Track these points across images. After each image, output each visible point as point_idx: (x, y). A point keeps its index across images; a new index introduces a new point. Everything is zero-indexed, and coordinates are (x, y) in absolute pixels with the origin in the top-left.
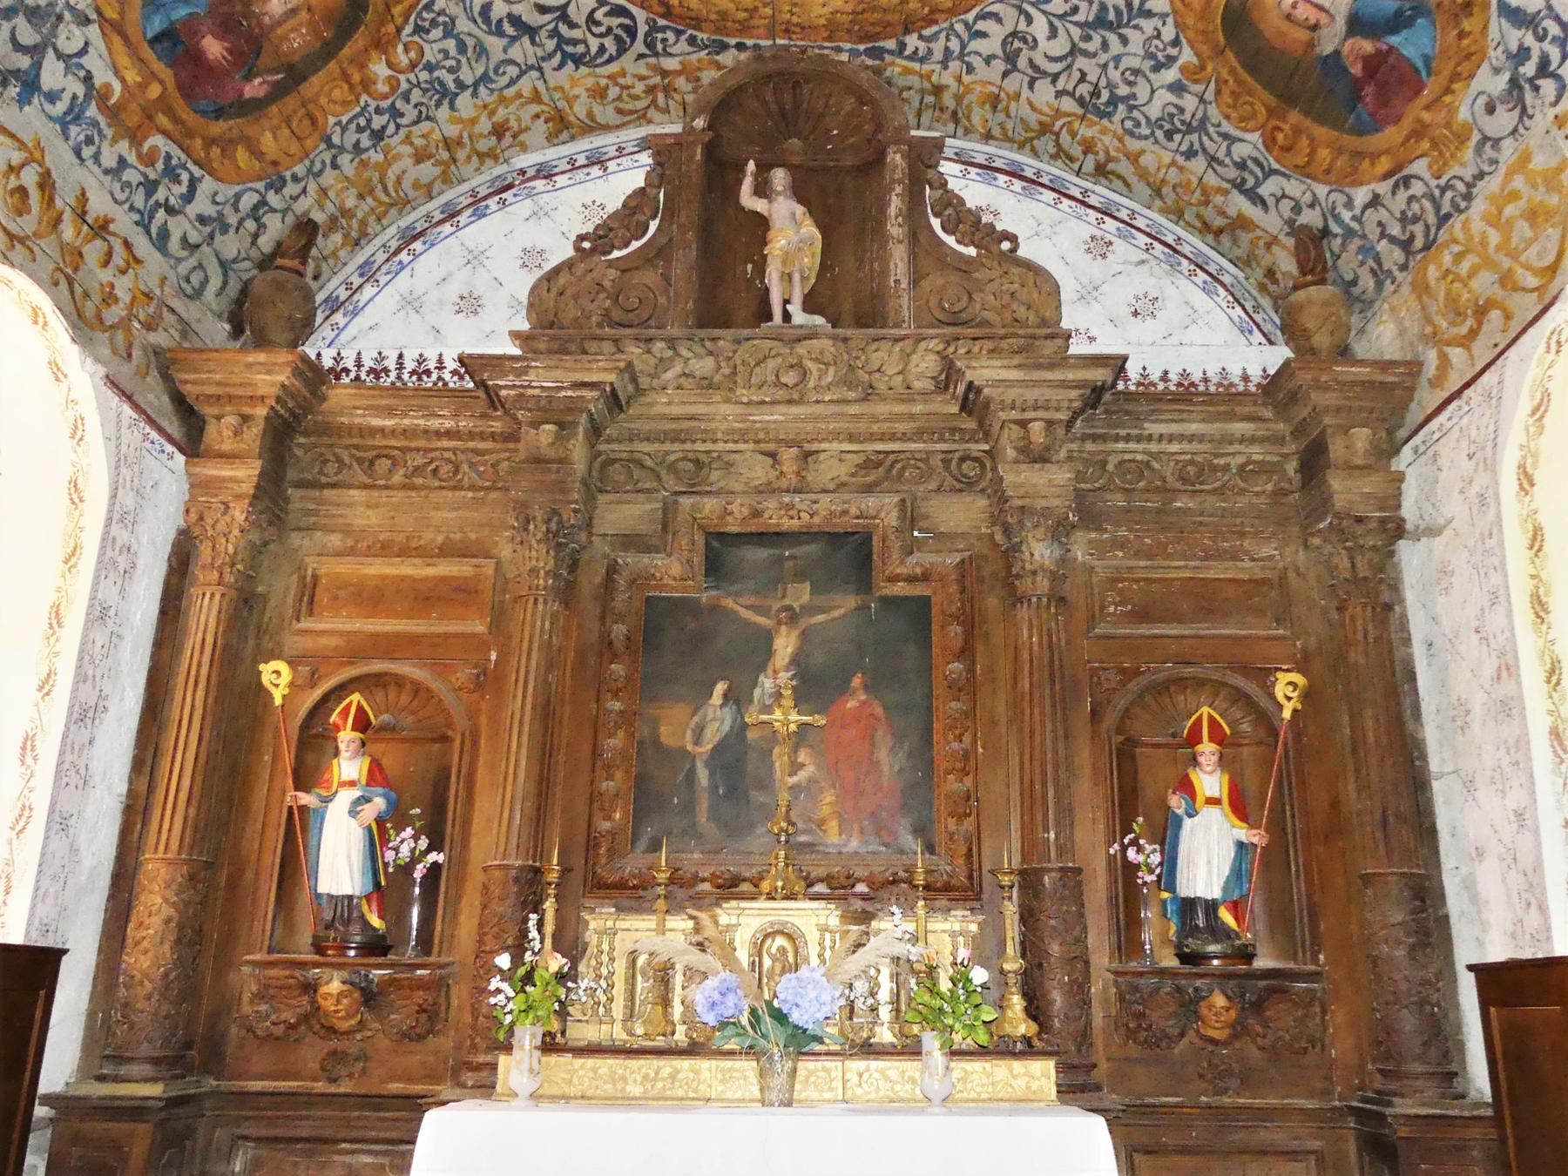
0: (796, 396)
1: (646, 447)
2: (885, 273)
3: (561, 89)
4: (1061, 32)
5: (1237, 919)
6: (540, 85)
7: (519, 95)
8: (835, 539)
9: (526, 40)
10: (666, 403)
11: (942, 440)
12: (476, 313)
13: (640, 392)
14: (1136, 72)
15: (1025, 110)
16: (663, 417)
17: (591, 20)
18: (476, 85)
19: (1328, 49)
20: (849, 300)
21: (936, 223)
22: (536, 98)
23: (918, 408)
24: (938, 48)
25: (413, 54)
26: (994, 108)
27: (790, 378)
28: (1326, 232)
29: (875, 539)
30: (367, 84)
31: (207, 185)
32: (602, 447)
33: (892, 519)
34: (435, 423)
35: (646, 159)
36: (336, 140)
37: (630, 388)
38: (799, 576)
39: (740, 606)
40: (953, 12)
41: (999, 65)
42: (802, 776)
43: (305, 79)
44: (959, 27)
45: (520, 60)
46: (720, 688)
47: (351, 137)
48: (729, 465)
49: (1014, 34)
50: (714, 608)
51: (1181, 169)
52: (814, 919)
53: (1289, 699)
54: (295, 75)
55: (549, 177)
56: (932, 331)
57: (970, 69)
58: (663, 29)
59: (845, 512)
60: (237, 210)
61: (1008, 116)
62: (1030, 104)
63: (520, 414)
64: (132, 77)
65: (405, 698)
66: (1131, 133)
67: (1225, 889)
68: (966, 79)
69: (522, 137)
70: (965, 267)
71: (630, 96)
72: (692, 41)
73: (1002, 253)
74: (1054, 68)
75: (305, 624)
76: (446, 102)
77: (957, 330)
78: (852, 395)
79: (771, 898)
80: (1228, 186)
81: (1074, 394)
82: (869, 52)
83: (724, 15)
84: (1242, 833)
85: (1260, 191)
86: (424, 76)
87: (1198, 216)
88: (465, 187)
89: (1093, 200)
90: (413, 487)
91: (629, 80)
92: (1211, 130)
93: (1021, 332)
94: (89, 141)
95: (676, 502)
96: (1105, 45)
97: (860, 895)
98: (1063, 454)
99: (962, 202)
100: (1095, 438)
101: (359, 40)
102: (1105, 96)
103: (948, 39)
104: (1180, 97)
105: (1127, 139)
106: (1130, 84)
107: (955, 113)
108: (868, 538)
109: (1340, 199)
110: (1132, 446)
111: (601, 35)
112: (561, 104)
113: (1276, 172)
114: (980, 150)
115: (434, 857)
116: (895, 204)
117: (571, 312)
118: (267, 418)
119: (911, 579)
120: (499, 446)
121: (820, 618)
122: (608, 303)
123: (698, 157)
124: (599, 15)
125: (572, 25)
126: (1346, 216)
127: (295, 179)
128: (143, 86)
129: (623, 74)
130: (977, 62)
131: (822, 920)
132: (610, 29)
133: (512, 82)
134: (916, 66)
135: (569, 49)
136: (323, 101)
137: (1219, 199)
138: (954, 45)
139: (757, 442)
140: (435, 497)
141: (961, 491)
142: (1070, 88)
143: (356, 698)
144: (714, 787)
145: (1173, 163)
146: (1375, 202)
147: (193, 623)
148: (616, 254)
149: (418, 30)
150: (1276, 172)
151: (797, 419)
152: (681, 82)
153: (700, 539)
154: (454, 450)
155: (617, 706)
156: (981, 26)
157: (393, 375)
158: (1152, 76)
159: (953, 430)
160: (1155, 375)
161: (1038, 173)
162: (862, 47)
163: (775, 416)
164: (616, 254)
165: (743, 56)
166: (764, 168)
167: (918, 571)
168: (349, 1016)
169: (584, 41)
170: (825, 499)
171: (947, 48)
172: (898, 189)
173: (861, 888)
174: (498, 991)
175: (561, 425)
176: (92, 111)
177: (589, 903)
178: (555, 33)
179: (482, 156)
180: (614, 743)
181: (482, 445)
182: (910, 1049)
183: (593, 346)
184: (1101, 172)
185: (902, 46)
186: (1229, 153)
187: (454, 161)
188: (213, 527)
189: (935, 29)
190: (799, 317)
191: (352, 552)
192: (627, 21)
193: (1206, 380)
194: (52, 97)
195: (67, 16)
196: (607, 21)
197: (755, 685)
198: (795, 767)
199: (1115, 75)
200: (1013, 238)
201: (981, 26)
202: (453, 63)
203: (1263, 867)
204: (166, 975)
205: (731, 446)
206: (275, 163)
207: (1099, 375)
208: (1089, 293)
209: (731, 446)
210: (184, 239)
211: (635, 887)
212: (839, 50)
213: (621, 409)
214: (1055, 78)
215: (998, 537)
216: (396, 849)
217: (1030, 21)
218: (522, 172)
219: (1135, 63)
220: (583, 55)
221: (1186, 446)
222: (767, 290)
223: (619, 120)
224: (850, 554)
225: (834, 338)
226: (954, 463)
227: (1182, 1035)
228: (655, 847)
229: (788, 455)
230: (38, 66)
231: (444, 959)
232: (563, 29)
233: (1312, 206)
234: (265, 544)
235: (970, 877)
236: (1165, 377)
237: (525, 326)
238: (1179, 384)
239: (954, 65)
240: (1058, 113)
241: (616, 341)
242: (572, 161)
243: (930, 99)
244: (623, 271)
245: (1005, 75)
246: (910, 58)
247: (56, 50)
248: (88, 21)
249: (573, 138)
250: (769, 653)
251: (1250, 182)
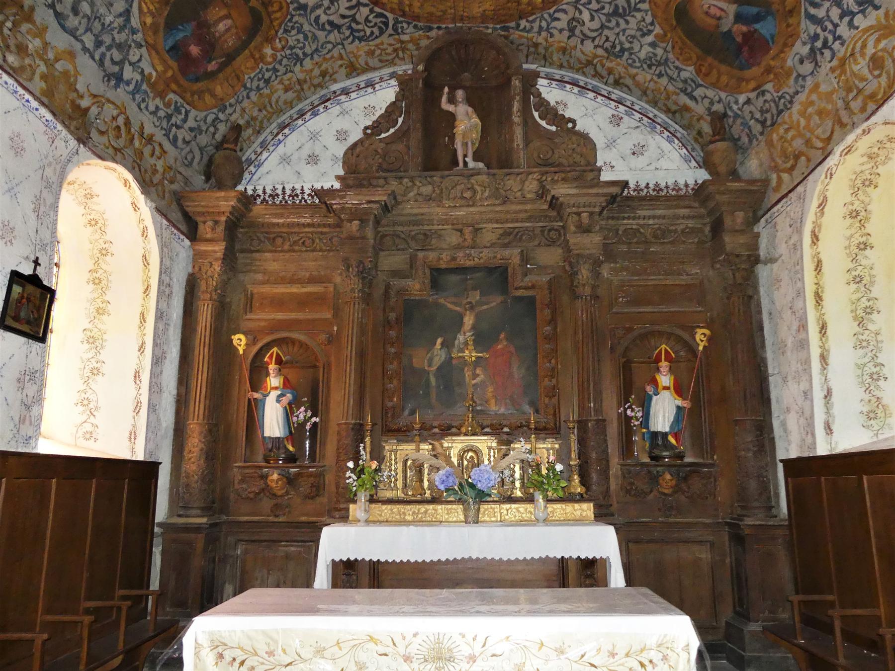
0: (471, 203)
1: (399, 228)
2: (512, 141)
3: (353, 52)
4: (596, 18)
5: (676, 440)
6: (343, 52)
7: (332, 57)
8: (490, 270)
9: (336, 31)
10: (410, 208)
11: (540, 221)
12: (316, 163)
13: (397, 203)
14: (633, 37)
15: (579, 54)
16: (410, 215)
17: (367, 20)
18: (312, 54)
19: (725, 29)
20: (495, 156)
21: (536, 114)
22: (341, 58)
23: (529, 207)
24: (536, 25)
25: (283, 43)
26: (564, 53)
27: (468, 194)
28: (725, 115)
29: (509, 269)
30: (262, 58)
31: (193, 113)
32: (379, 229)
33: (516, 260)
34: (302, 220)
35: (393, 82)
36: (248, 85)
37: (393, 202)
38: (474, 289)
39: (448, 303)
40: (543, 9)
41: (566, 33)
42: (478, 380)
43: (234, 59)
44: (546, 16)
45: (333, 41)
46: (439, 341)
47: (255, 84)
48: (440, 235)
49: (573, 19)
50: (437, 305)
51: (656, 82)
52: (485, 444)
53: (702, 341)
54: (230, 58)
55: (347, 94)
56: (535, 170)
57: (552, 35)
58: (402, 22)
59: (495, 257)
60: (206, 123)
61: (571, 57)
62: (582, 51)
63: (342, 216)
64: (160, 68)
65: (296, 349)
66: (631, 65)
67: (671, 427)
68: (550, 40)
69: (333, 77)
70: (550, 136)
71: (386, 54)
72: (415, 27)
73: (568, 129)
74: (594, 34)
75: (249, 316)
76: (298, 64)
77: (547, 169)
78: (498, 202)
79: (466, 435)
80: (678, 91)
81: (603, 199)
82: (501, 28)
83: (431, 14)
84: (679, 402)
85: (694, 94)
86: (288, 52)
87: (665, 105)
88: (308, 101)
89: (613, 97)
90: (294, 251)
91: (385, 46)
92: (670, 64)
93: (577, 169)
94: (144, 100)
95: (416, 255)
96: (618, 24)
97: (506, 433)
98: (597, 228)
99: (548, 103)
100: (613, 218)
101: (258, 39)
102: (618, 48)
103: (541, 21)
104: (655, 49)
105: (629, 68)
106: (631, 43)
107: (545, 57)
108: (506, 269)
109: (732, 99)
110: (630, 221)
111: (372, 27)
112: (353, 60)
113: (701, 85)
114: (558, 73)
115: (314, 419)
116: (516, 106)
117: (363, 165)
118: (226, 222)
119: (526, 288)
120: (332, 230)
121: (485, 307)
122: (380, 160)
123: (420, 85)
124: (371, 17)
125: (358, 23)
126: (735, 107)
127: (231, 105)
128: (165, 72)
129: (382, 44)
130: (555, 32)
131: (489, 444)
132: (376, 24)
133: (330, 51)
134: (526, 34)
135: (357, 34)
136: (243, 68)
137: (674, 97)
138: (544, 24)
139: (453, 224)
140: (304, 255)
141: (550, 245)
142: (601, 44)
143: (275, 349)
144: (438, 387)
145: (652, 80)
146: (748, 102)
147: (200, 318)
148: (383, 135)
149: (286, 31)
150: (701, 85)
151: (471, 212)
152: (410, 46)
153: (427, 271)
154: (312, 233)
155: (393, 350)
156: (557, 15)
157: (281, 197)
158: (641, 40)
159: (546, 216)
160: (643, 185)
161: (586, 83)
162: (498, 26)
163: (461, 213)
164: (383, 135)
165: (440, 32)
166: (452, 90)
167: (530, 284)
168: (283, 489)
169: (363, 30)
170: (486, 251)
171: (540, 26)
172: (518, 98)
173: (506, 430)
174: (350, 477)
175: (361, 221)
176: (144, 87)
177: (385, 438)
178: (350, 27)
179: (315, 86)
180: (392, 367)
181: (325, 230)
182: (529, 499)
183: (374, 182)
184: (617, 83)
185: (518, 25)
186: (679, 76)
187: (303, 89)
188: (206, 273)
189: (534, 17)
190: (471, 164)
191: (267, 282)
192: (384, 20)
193: (667, 187)
194: (128, 83)
195: (133, 45)
196: (374, 20)
197: (455, 338)
198: (475, 376)
199: (623, 39)
200: (574, 122)
201: (557, 15)
202: (302, 45)
204: (202, 473)
205: (440, 227)
206: (222, 100)
207: (614, 190)
208: (611, 144)
209: (440, 227)
210: (184, 139)
211: (405, 431)
212: (487, 28)
213: (389, 211)
214: (594, 39)
215: (567, 268)
216: (297, 416)
217: (581, 12)
218: (335, 92)
219: (633, 32)
220: (363, 36)
221: (656, 221)
222: (456, 150)
223: (380, 65)
224: (498, 276)
225: (488, 174)
226: (546, 232)
227: (651, 491)
228: (413, 413)
229: (467, 231)
230: (122, 70)
231: (321, 464)
232: (354, 25)
233: (719, 102)
234: (229, 279)
235: (555, 424)
236: (647, 186)
237: (341, 172)
238: (654, 190)
239: (544, 34)
240: (596, 56)
241: (385, 178)
242: (358, 86)
243: (532, 49)
244: (387, 144)
245: (569, 38)
246: (521, 31)
247: (129, 62)
248: (141, 46)
249: (358, 75)
250: (461, 324)
251: (689, 90)
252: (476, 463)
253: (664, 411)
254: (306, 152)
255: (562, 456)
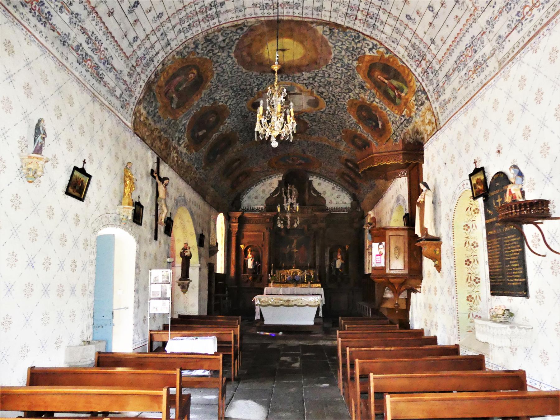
52: (298, 270)
97: (303, 268)
182: (307, 283)
203: (345, 265)
252: (296, 275)
253: (339, 264)
254: (254, 196)
255: (315, 274)
